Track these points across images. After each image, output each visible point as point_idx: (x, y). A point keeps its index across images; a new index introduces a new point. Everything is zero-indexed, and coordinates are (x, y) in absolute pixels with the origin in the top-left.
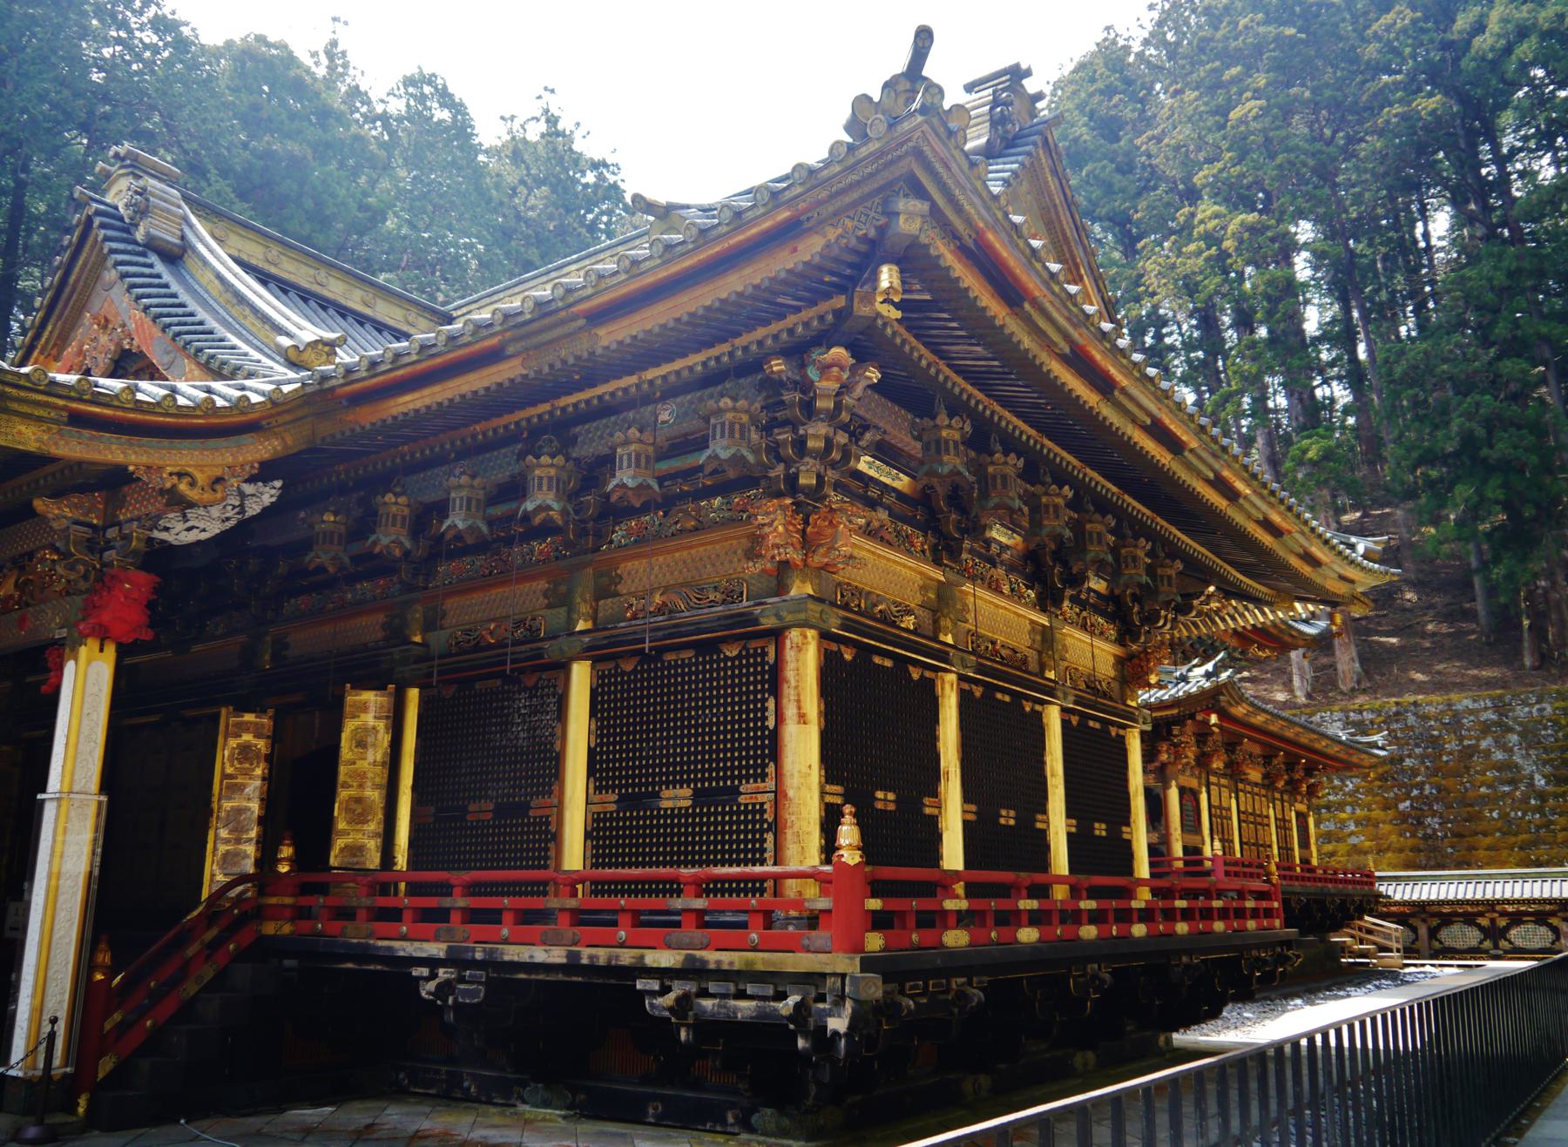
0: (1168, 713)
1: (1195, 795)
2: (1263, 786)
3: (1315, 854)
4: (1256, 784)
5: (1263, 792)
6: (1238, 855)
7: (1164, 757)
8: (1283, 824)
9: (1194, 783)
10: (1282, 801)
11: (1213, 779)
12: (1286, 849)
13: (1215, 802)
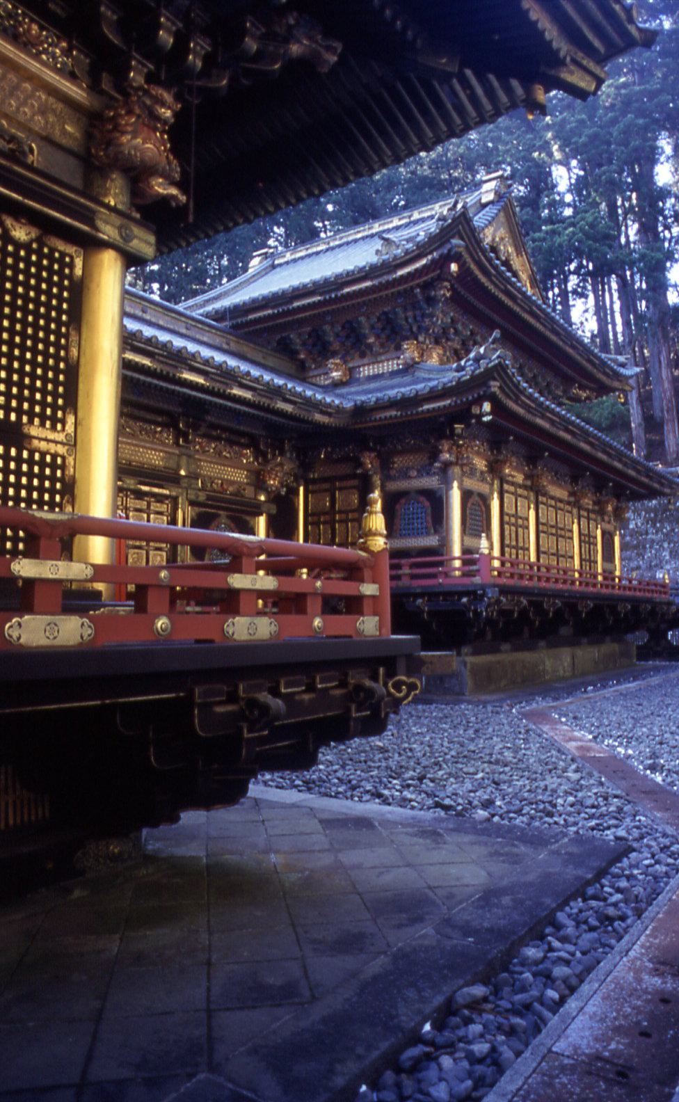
0: (441, 404)
1: (485, 500)
2: (569, 503)
3: (618, 568)
4: (561, 501)
5: (568, 508)
6: (533, 558)
7: (446, 456)
8: (587, 539)
9: (484, 488)
10: (588, 519)
11: (506, 487)
12: (588, 560)
13: (509, 509)
